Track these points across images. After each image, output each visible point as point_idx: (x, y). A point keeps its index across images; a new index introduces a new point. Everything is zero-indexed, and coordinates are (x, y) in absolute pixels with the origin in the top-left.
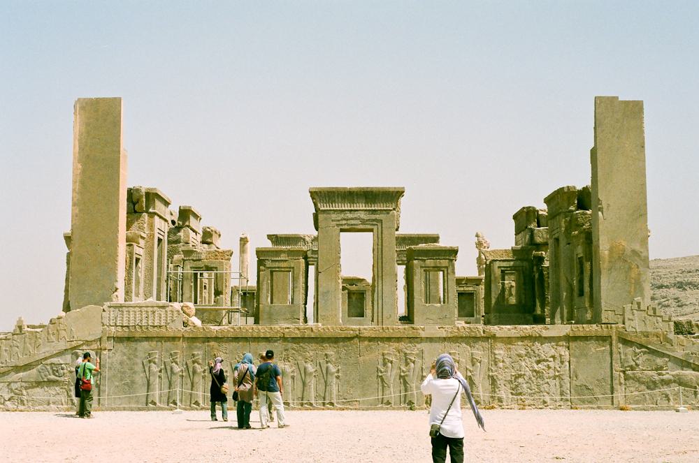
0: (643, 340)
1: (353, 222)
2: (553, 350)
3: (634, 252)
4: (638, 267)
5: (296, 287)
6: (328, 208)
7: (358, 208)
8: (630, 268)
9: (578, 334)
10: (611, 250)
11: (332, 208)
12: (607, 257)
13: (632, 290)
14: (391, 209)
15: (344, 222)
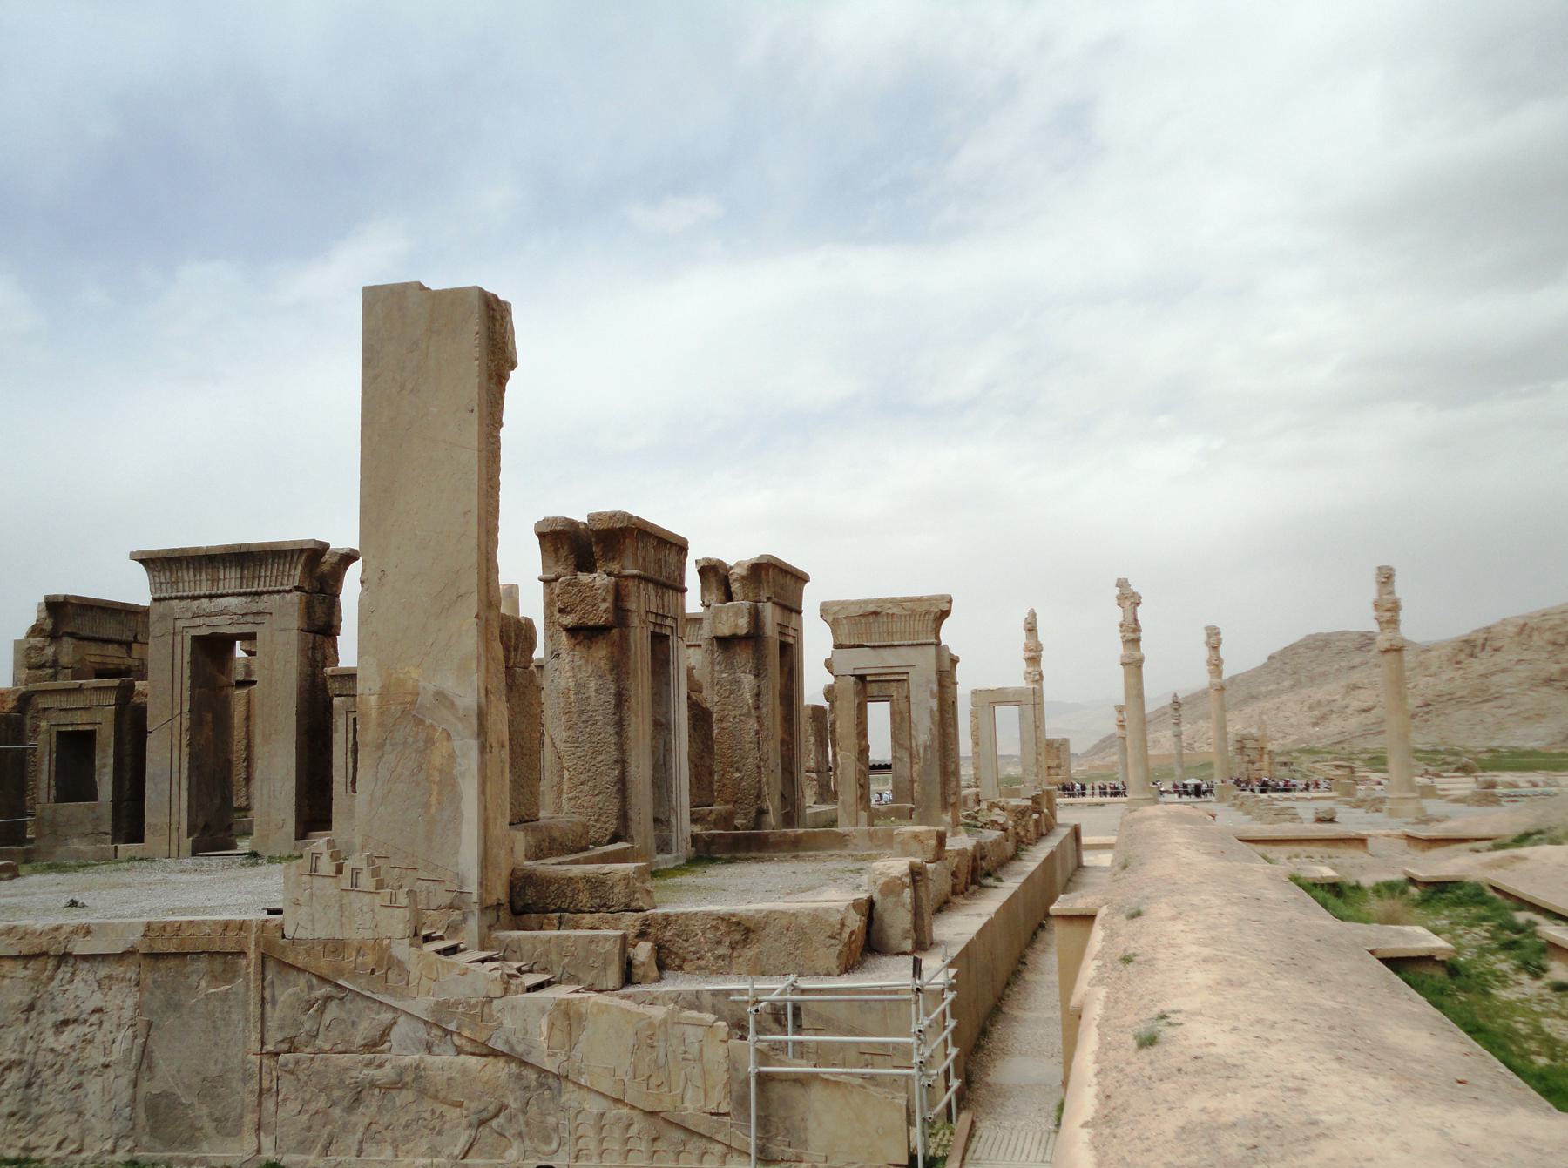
0: (324, 965)
1: (216, 621)
2: (98, 995)
3: (440, 696)
4: (449, 737)
5: (104, 766)
6: (168, 596)
7: (225, 591)
8: (430, 741)
9: (159, 947)
10: (384, 694)
11: (174, 595)
12: (374, 713)
13: (433, 800)
14: (287, 588)
15: (198, 621)
